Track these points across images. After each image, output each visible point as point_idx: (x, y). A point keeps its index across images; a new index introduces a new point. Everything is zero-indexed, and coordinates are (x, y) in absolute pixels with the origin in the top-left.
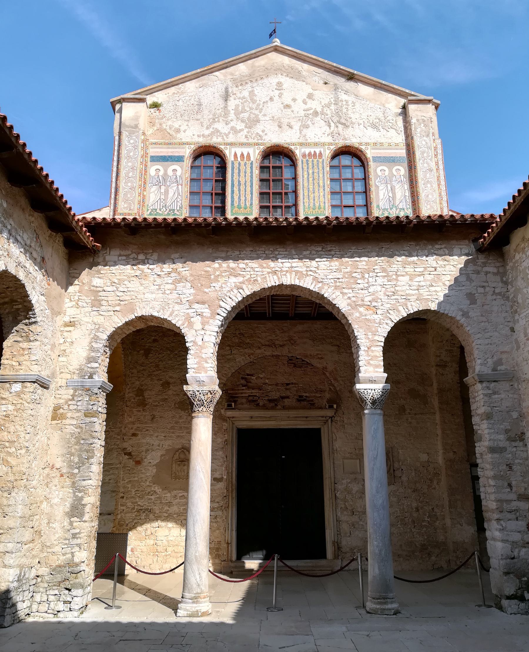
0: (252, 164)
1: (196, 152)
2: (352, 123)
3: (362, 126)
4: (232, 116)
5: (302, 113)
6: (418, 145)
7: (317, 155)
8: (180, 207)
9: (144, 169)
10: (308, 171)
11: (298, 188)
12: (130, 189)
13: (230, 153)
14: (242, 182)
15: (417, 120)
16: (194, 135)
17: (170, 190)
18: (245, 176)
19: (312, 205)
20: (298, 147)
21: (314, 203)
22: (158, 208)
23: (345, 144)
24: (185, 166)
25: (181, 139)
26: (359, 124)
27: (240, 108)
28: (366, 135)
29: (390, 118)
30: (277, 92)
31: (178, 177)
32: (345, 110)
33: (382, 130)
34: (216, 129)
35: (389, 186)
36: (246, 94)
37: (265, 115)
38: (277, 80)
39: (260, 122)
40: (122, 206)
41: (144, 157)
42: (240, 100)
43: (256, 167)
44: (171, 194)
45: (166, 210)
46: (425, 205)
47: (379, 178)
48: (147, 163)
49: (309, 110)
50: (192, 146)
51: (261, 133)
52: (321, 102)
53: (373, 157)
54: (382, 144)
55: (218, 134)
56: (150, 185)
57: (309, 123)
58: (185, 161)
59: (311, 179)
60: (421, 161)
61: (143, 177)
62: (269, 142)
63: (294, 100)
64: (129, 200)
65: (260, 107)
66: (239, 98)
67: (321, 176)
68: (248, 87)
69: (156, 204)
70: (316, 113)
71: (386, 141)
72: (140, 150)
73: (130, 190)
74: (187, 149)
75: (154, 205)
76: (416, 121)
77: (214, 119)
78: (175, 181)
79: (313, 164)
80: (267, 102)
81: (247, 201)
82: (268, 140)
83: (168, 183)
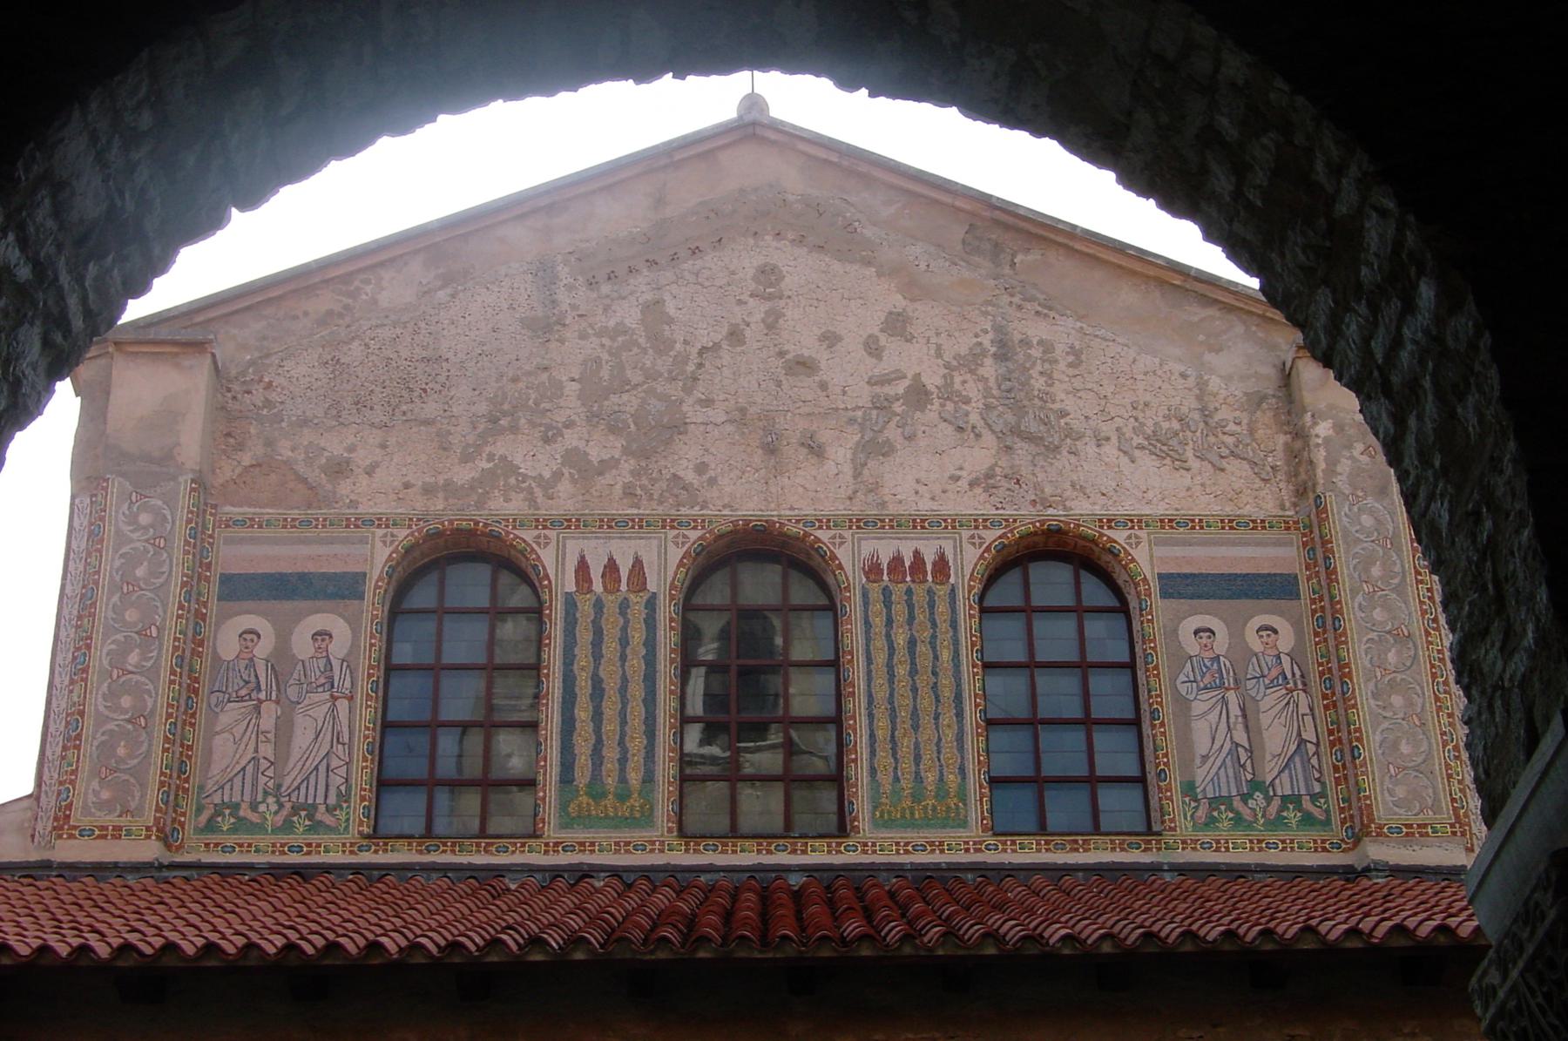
0: (651, 604)
1: (417, 554)
2: (1069, 433)
3: (1110, 450)
4: (571, 405)
5: (862, 395)
6: (1345, 530)
7: (929, 568)
8: (339, 794)
9: (190, 634)
10: (888, 636)
11: (849, 705)
12: (129, 721)
13: (560, 559)
14: (611, 685)
15: (1334, 426)
16: (407, 486)
17: (299, 720)
18: (623, 658)
19: (907, 783)
20: (847, 534)
21: (917, 773)
22: (247, 798)
23: (1042, 523)
24: (366, 618)
25: (354, 504)
26: (1100, 441)
27: (605, 373)
28: (1127, 484)
29: (1224, 414)
30: (758, 310)
31: (336, 664)
32: (1042, 380)
33: (1194, 464)
34: (503, 458)
35: (1232, 696)
36: (629, 314)
37: (708, 402)
38: (759, 260)
39: (686, 433)
40: (91, 798)
41: (195, 583)
42: (606, 341)
43: (671, 620)
44: (302, 738)
45: (281, 806)
46: (1387, 784)
47: (1188, 664)
48: (205, 605)
49: (889, 382)
50: (402, 533)
51: (690, 476)
52: (939, 347)
53: (1160, 576)
54: (1192, 523)
55: (512, 481)
56: (213, 700)
57: (892, 433)
58: (369, 595)
59: (902, 671)
60: (1359, 598)
61: (186, 668)
62: (726, 512)
63: (830, 339)
64: (124, 771)
65: (691, 368)
66: (599, 335)
67: (945, 655)
68: (641, 286)
69: (238, 781)
70: (918, 395)
71: (1216, 509)
72: (178, 554)
73: (130, 727)
74: (379, 545)
75: (227, 787)
76: (1331, 432)
77: (495, 421)
78: (323, 681)
79: (911, 607)
80: (716, 347)
81: (630, 765)
82: (720, 503)
83: (292, 693)
